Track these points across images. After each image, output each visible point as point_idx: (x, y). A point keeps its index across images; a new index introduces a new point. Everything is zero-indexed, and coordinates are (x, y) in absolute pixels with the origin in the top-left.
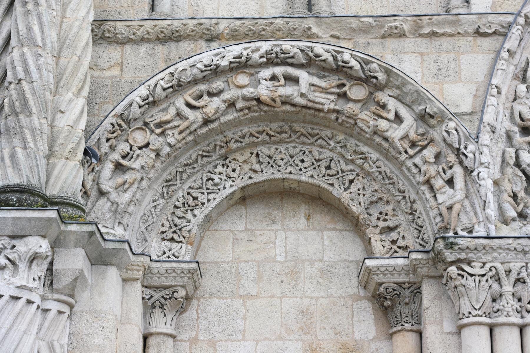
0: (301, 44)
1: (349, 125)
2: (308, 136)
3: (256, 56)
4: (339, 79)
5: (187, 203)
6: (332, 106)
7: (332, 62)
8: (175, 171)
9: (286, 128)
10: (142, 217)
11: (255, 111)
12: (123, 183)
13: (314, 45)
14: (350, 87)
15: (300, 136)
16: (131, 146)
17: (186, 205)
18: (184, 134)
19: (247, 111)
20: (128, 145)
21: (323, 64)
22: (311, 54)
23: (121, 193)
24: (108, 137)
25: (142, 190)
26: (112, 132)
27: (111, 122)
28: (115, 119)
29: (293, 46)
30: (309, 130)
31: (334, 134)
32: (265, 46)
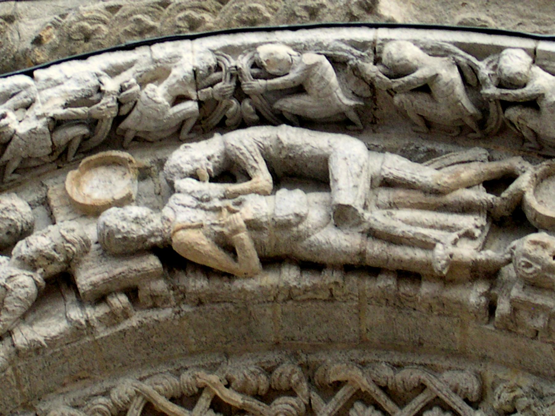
0: (328, 37)
1: (540, 323)
2: (382, 399)
3: (158, 93)
4: (490, 159)
6: (467, 251)
7: (459, 89)
9: (289, 372)
11: (156, 301)
13: (383, 33)
14: (540, 180)
15: (349, 405)
19: (124, 299)
21: (421, 102)
22: (371, 69)
29: (301, 48)
30: (385, 373)
31: (489, 380)
32: (192, 56)
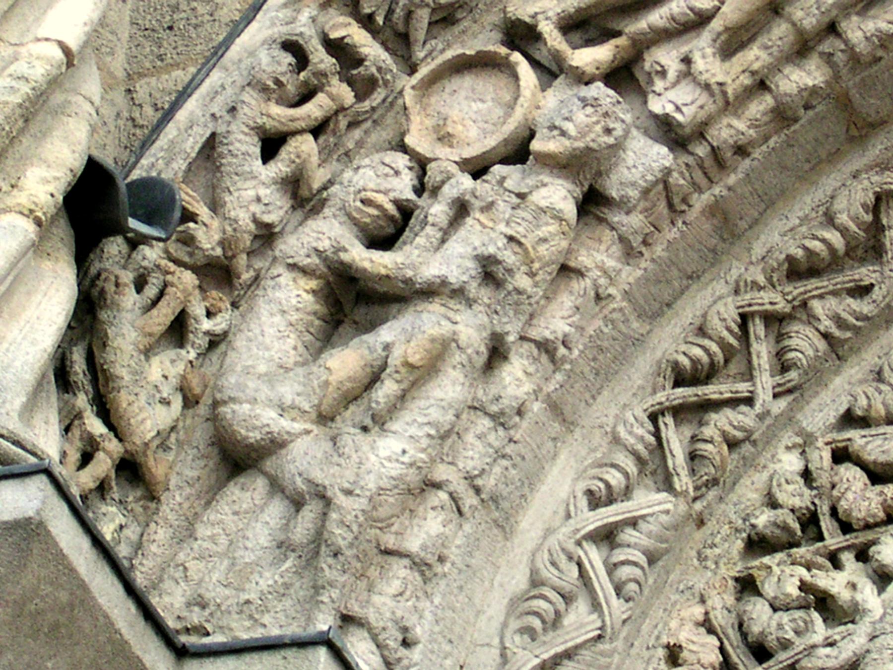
5: (834, 512)
8: (729, 310)
10: (514, 602)
12: (363, 376)
16: (421, 164)
17: (826, 524)
18: (755, 56)
20: (401, 161)
23: (350, 437)
24: (269, 124)
25: (499, 419)
26: (291, 89)
27: (281, 31)
28: (304, 16)
